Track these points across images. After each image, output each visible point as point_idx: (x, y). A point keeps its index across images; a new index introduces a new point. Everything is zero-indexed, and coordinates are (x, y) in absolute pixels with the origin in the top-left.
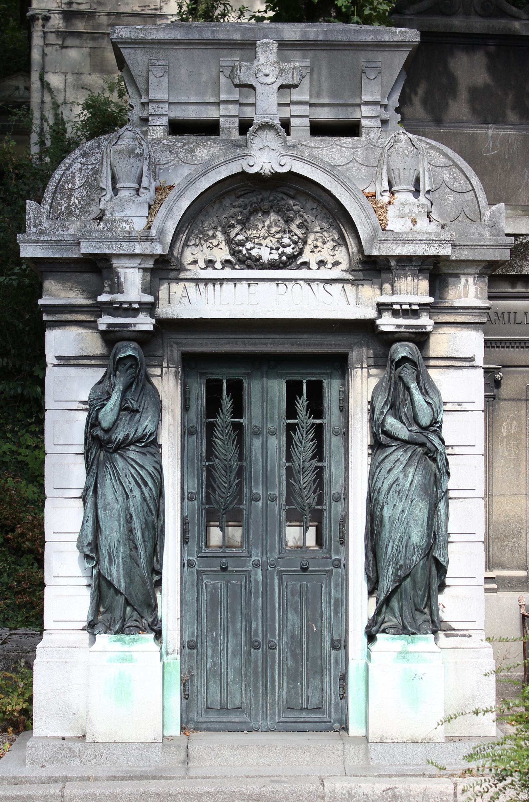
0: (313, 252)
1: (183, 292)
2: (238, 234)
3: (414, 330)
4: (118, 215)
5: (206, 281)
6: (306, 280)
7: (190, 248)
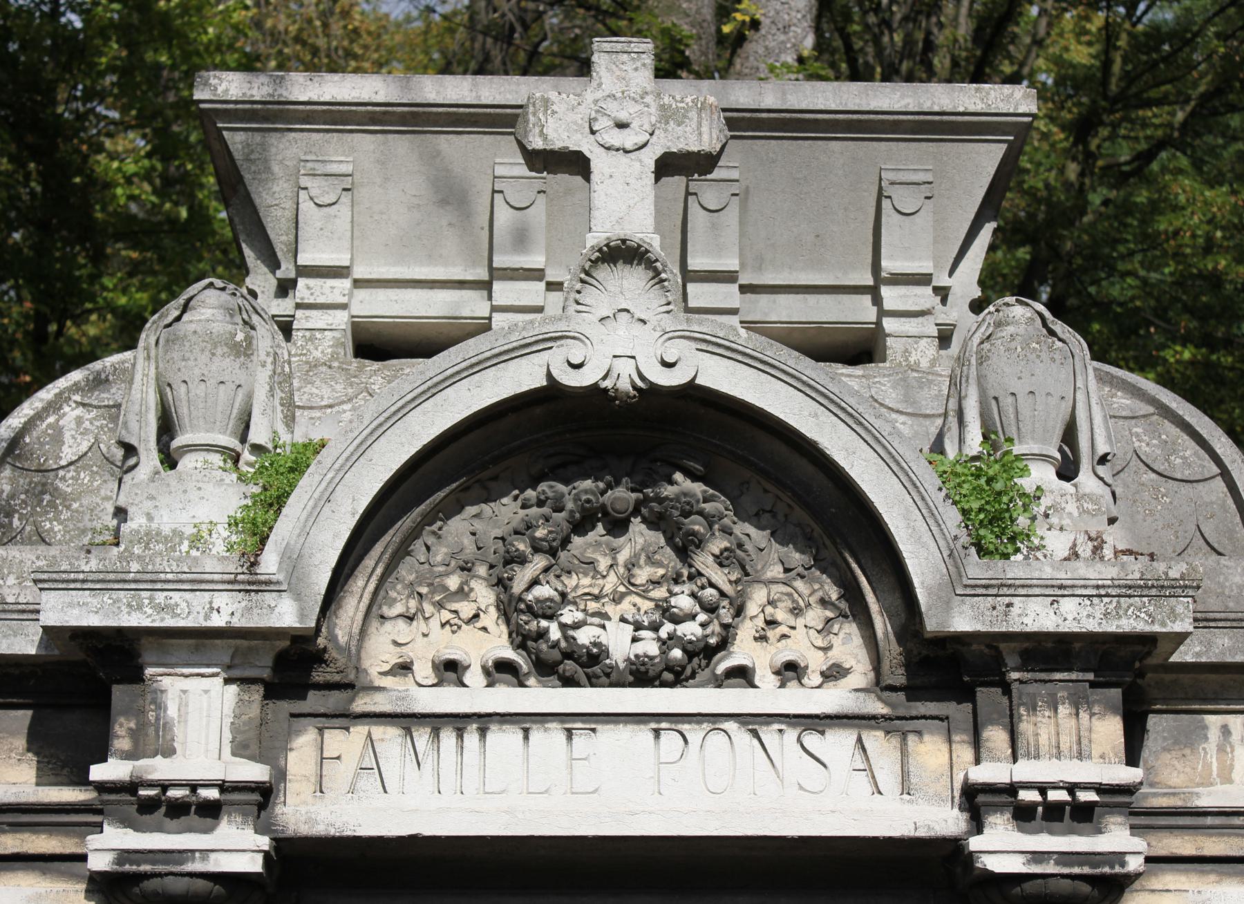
0: (762, 638)
1: (362, 757)
2: (535, 582)
3: (1086, 870)
4: (166, 521)
5: (436, 721)
6: (743, 719)
7: (388, 626)
